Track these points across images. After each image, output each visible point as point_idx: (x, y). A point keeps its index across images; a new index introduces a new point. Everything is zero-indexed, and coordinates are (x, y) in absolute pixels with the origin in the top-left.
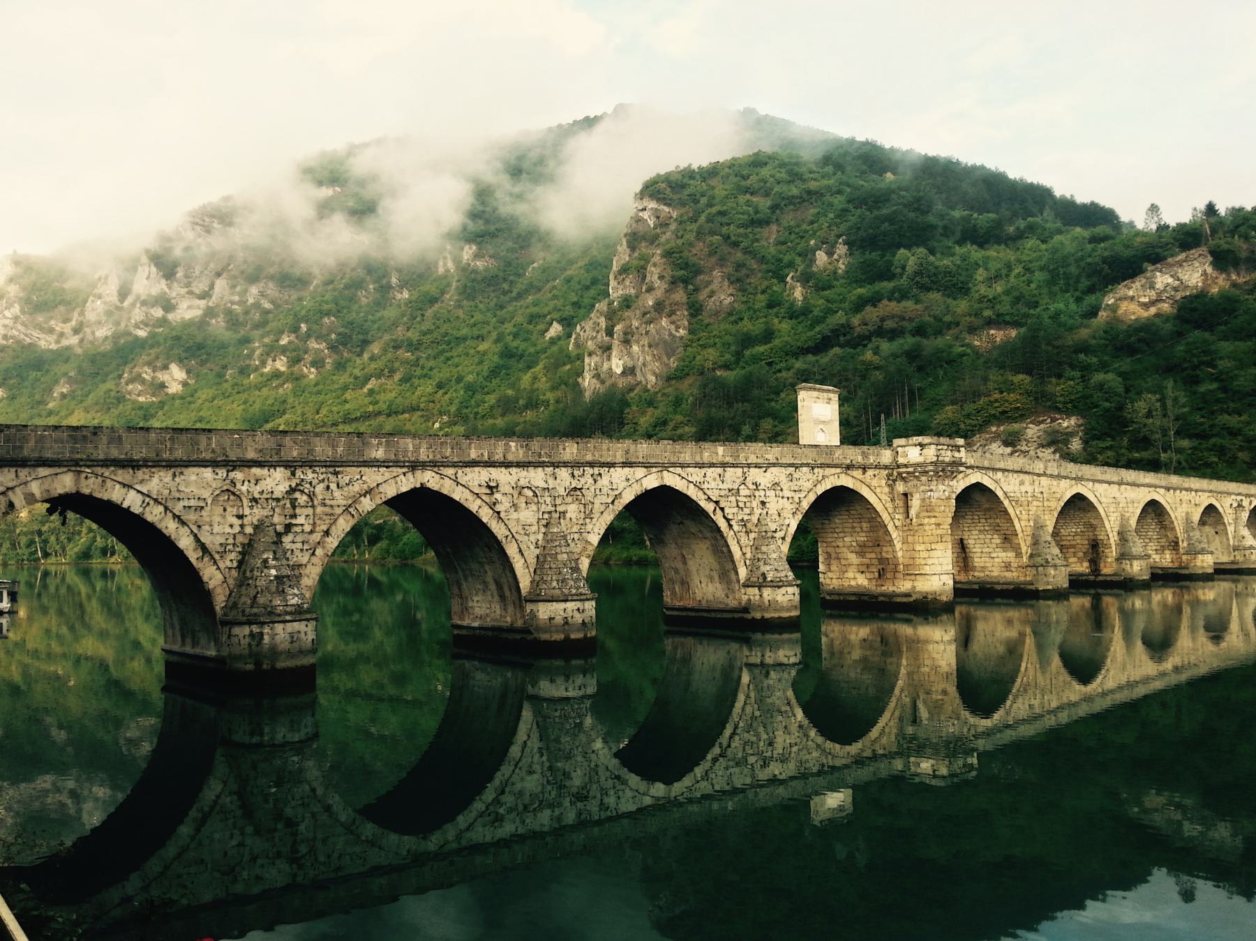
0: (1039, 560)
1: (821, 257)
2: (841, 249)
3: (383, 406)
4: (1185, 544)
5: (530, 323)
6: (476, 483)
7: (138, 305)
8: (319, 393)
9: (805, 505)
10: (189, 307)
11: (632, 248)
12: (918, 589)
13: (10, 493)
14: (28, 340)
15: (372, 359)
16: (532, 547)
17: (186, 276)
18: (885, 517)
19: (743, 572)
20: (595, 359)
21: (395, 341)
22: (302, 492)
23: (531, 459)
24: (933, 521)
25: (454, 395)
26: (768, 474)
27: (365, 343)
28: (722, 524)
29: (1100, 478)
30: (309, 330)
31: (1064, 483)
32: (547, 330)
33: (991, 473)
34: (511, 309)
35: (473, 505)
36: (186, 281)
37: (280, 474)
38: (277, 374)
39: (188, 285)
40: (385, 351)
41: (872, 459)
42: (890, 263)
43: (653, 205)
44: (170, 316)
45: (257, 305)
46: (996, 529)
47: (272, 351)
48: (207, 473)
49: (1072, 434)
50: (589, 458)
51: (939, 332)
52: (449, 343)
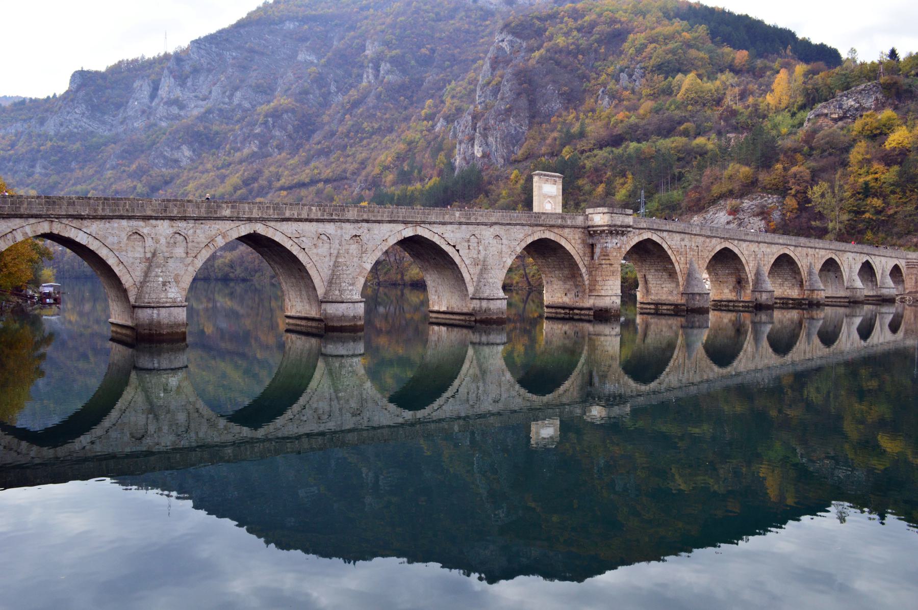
0: (690, 291)
4: (807, 284)
6: (290, 231)
7: (162, 105)
10: (196, 107)
11: (494, 67)
12: (596, 305)
13: (14, 232)
14: (91, 129)
16: (325, 270)
18: (577, 258)
19: (471, 290)
20: (463, 146)
22: (180, 234)
23: (325, 217)
24: (608, 262)
28: (457, 260)
29: (743, 238)
31: (714, 240)
33: (659, 233)
35: (288, 244)
37: (166, 223)
41: (569, 222)
42: (670, 83)
43: (509, 37)
44: (182, 113)
45: (239, 105)
46: (665, 270)
48: (124, 223)
49: (773, 209)
50: (365, 217)
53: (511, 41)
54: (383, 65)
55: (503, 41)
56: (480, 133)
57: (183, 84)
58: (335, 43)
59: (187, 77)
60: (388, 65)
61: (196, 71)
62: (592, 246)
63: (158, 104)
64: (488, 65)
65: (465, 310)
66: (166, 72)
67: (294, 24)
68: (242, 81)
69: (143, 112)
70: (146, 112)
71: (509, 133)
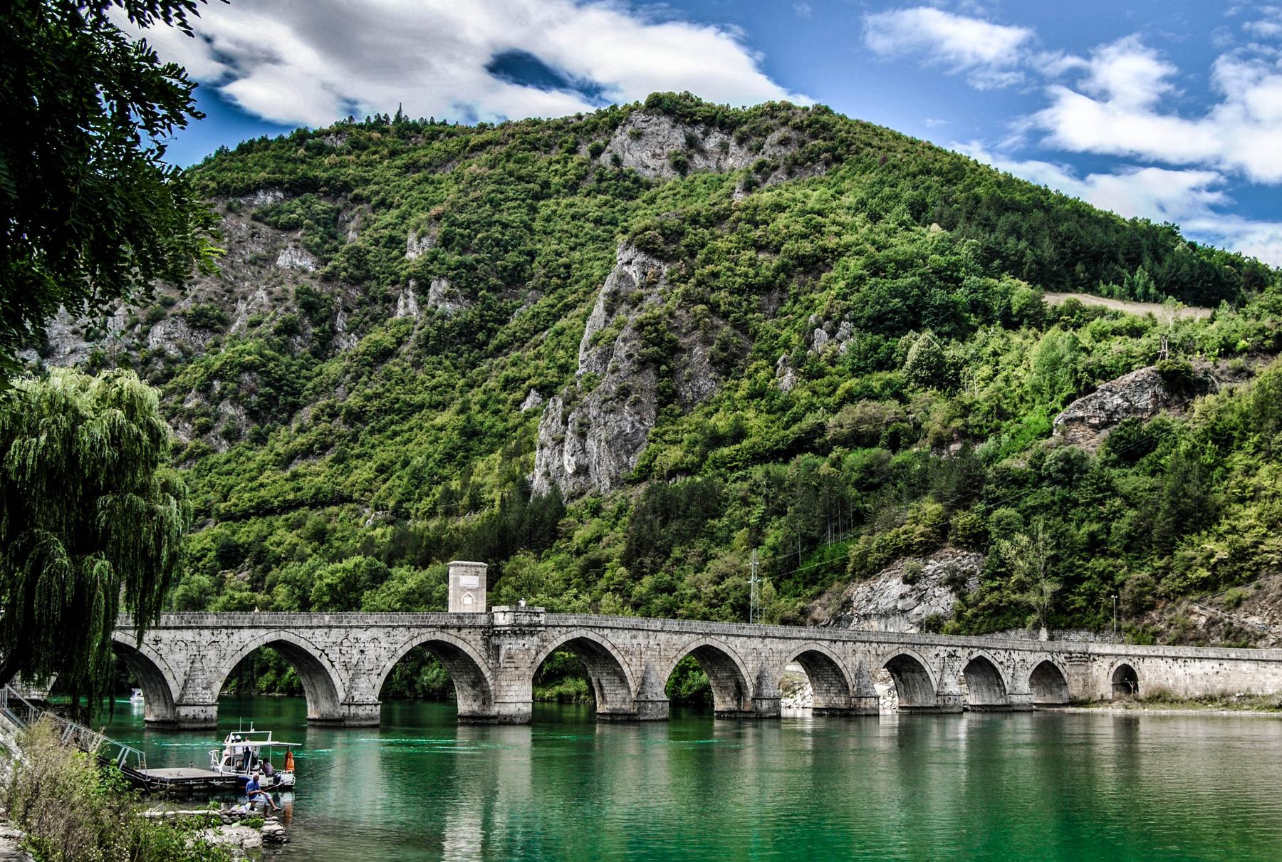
1: (821, 334)
3: (307, 493)
5: (504, 388)
8: (229, 473)
9: (401, 653)
11: (610, 311)
15: (301, 430)
18: (479, 661)
19: (341, 695)
20: (546, 452)
21: (331, 407)
25: (397, 482)
26: (368, 632)
27: (295, 408)
28: (326, 664)
29: (735, 632)
30: (224, 388)
31: (686, 638)
32: (524, 400)
34: (485, 367)
40: (317, 418)
41: (467, 622)
42: (893, 349)
43: (641, 258)
49: (972, 573)
50: (225, 624)
51: (913, 441)
52: (399, 411)
53: (644, 263)
54: (434, 284)
55: (629, 263)
56: (573, 432)
58: (351, 235)
60: (444, 283)
62: (498, 648)
64: (601, 304)
65: (337, 716)
71: (620, 433)
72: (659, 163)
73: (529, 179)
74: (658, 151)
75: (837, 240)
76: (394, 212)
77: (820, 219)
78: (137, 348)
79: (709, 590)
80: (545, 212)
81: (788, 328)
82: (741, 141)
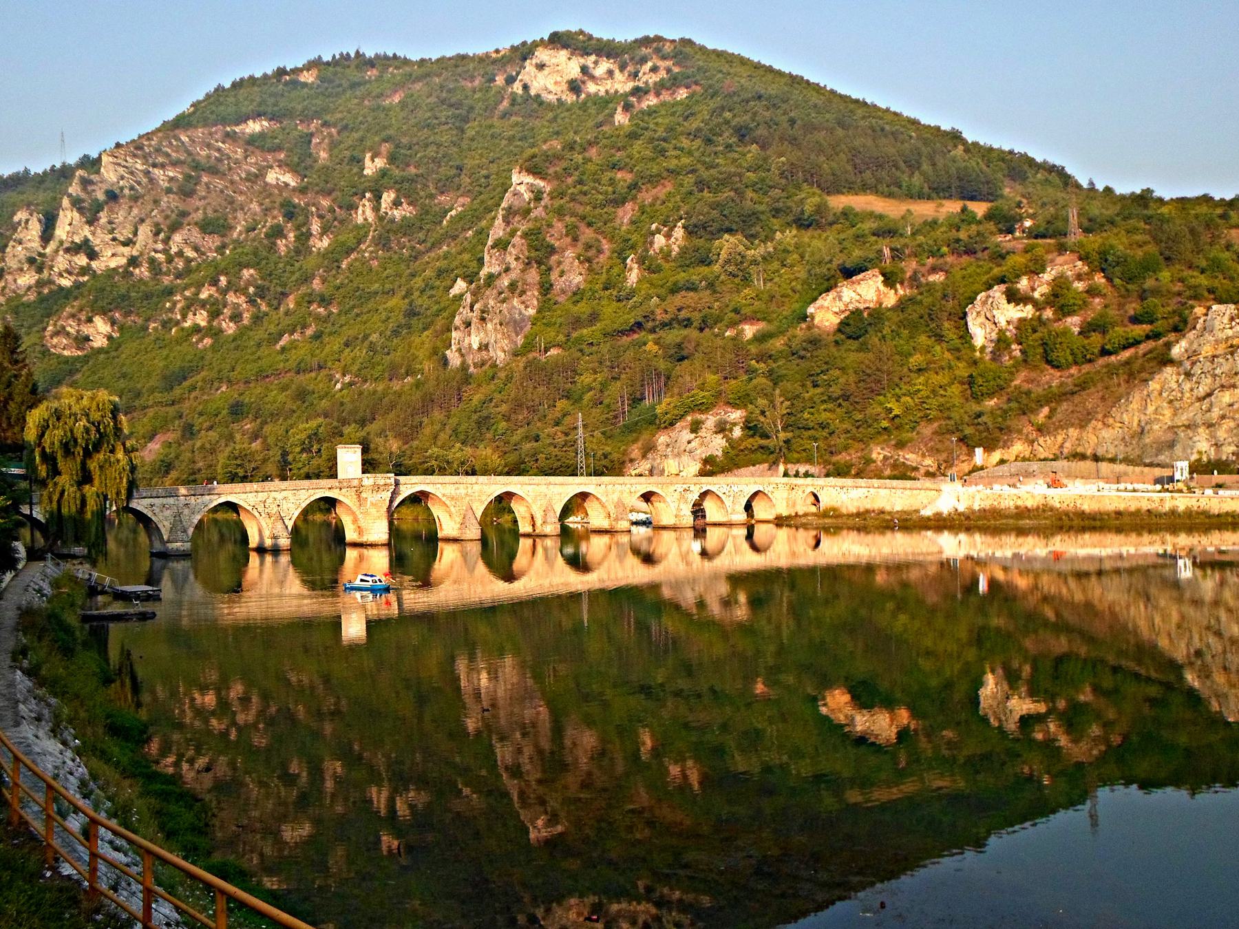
1: (660, 240)
2: (679, 232)
7: (61, 253)
9: (304, 505)
10: (113, 255)
11: (507, 221)
17: (110, 222)
27: (284, 295)
30: (229, 282)
35: (145, 511)
36: (109, 227)
38: (197, 329)
39: (112, 231)
44: (94, 264)
45: (180, 254)
47: (193, 304)
53: (532, 185)
54: (385, 195)
57: (91, 222)
59: (98, 207)
61: (112, 196)
63: (57, 251)
66: (66, 202)
67: (262, 126)
68: (184, 214)
69: (31, 261)
70: (36, 263)
72: (559, 89)
73: (457, 105)
74: (559, 79)
75: (676, 161)
76: (356, 135)
77: (664, 144)
78: (160, 252)
79: (560, 439)
80: (470, 133)
81: (636, 234)
82: (622, 68)
